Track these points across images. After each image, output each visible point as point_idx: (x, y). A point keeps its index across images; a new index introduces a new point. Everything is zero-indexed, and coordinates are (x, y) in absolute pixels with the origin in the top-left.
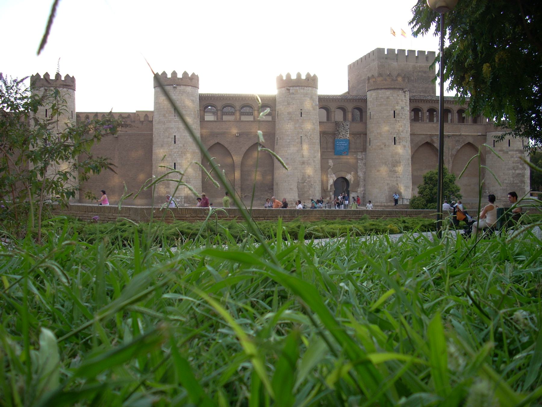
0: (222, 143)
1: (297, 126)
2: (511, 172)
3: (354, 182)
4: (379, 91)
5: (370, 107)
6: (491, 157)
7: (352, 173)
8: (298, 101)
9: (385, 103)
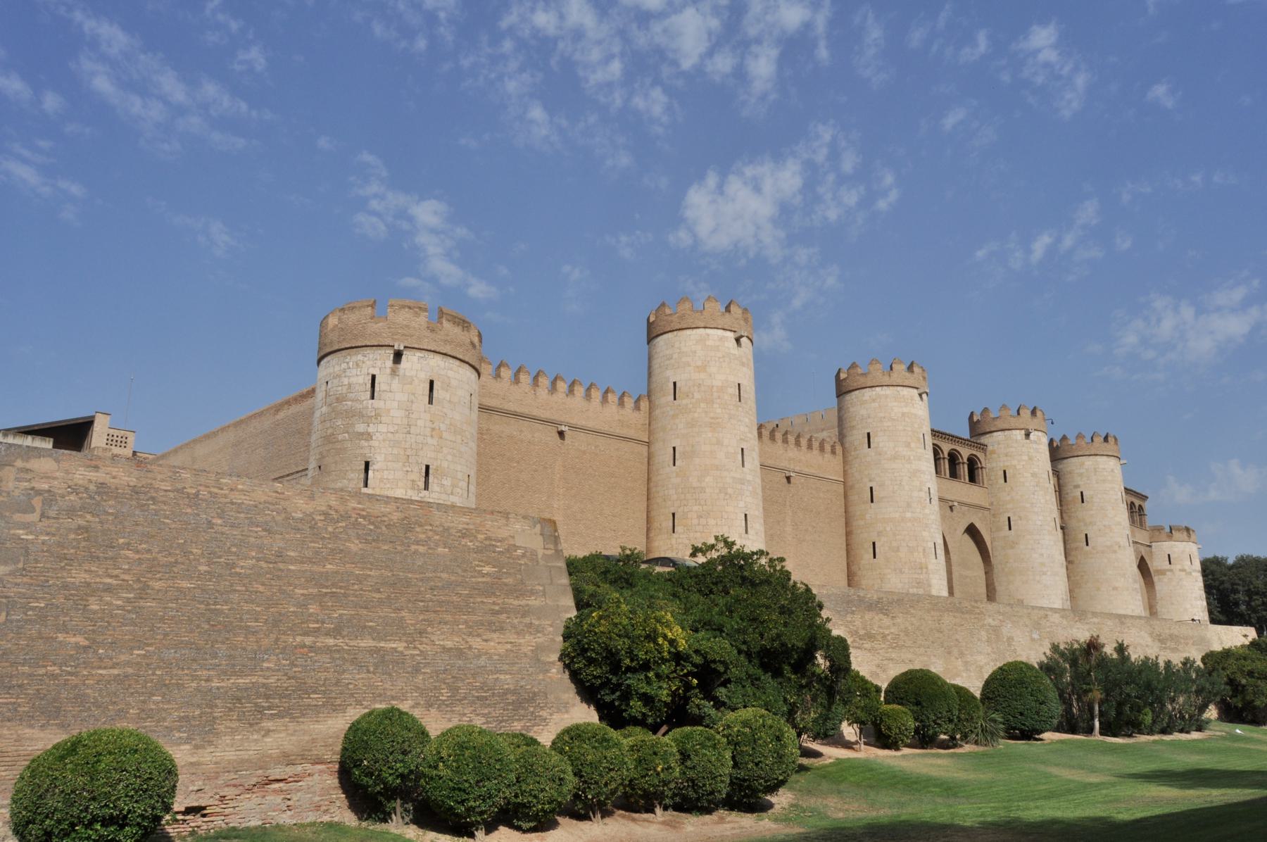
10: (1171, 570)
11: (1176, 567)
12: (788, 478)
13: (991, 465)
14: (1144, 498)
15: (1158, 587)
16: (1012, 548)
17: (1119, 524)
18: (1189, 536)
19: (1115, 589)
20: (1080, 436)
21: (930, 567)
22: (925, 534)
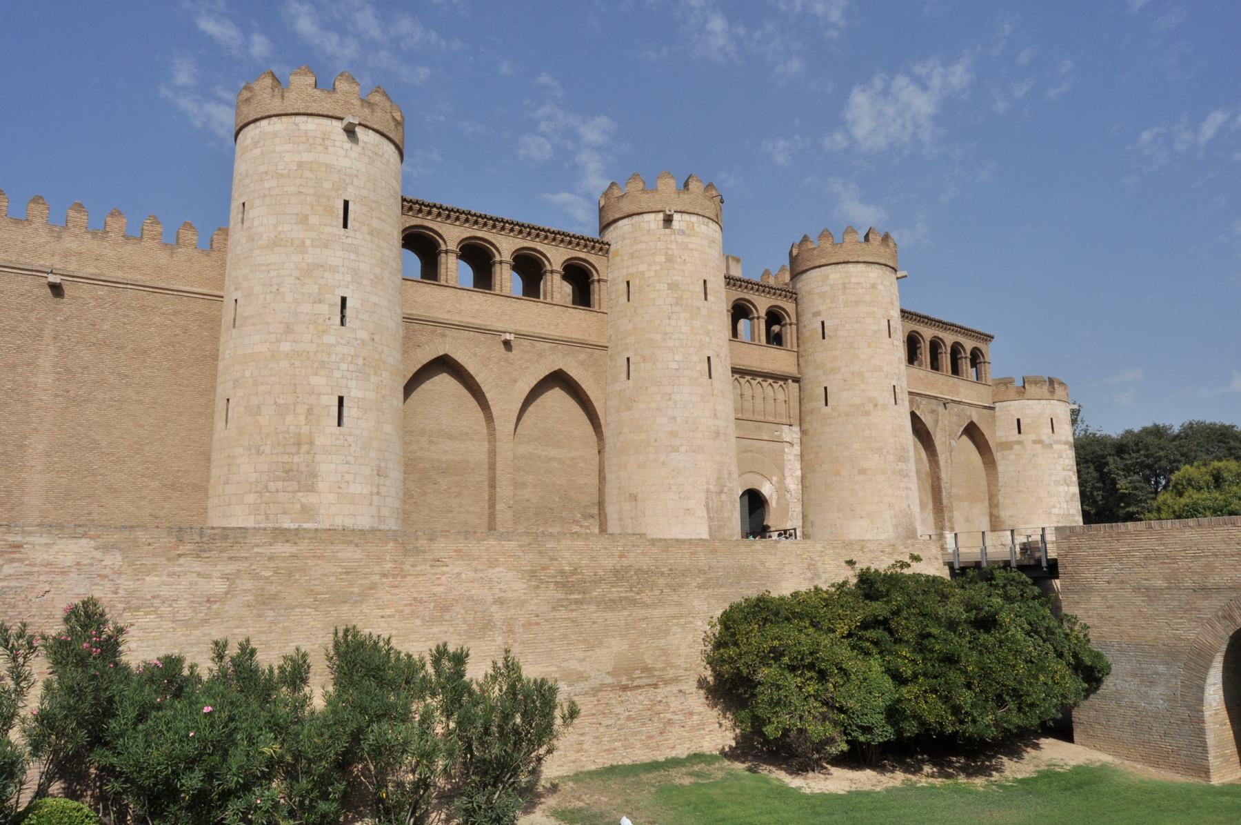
0: (460, 357)
1: (697, 324)
2: (1061, 489)
3: (777, 503)
4: (850, 267)
5: (821, 308)
6: (1012, 457)
7: (774, 479)
8: (696, 254)
9: (868, 298)
10: (1020, 443)
11: (1028, 437)
12: (57, 290)
13: (608, 275)
14: (988, 338)
15: (1001, 466)
16: (628, 408)
17: (879, 369)
18: (1052, 391)
19: (863, 471)
20: (825, 234)
21: (319, 441)
22: (319, 381)
